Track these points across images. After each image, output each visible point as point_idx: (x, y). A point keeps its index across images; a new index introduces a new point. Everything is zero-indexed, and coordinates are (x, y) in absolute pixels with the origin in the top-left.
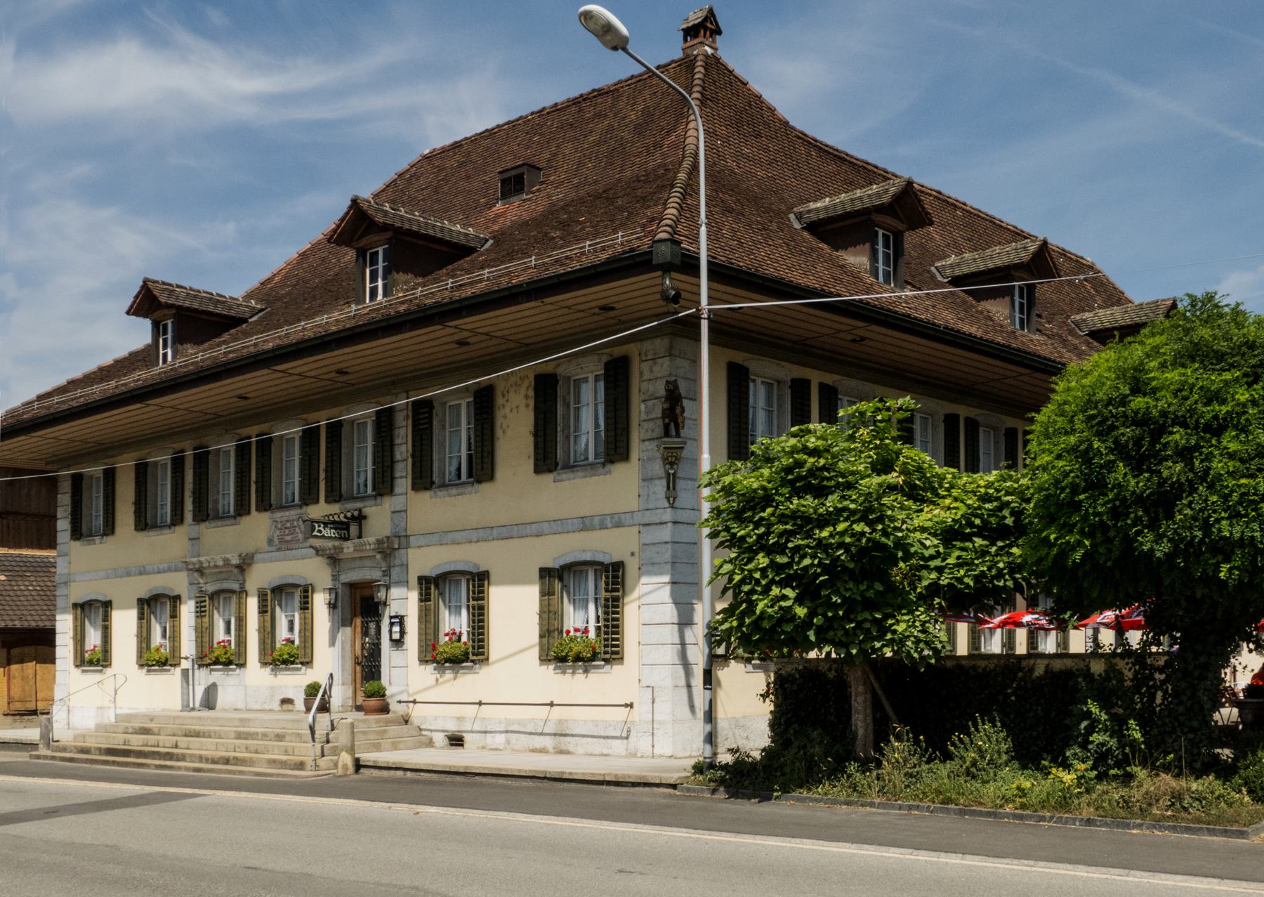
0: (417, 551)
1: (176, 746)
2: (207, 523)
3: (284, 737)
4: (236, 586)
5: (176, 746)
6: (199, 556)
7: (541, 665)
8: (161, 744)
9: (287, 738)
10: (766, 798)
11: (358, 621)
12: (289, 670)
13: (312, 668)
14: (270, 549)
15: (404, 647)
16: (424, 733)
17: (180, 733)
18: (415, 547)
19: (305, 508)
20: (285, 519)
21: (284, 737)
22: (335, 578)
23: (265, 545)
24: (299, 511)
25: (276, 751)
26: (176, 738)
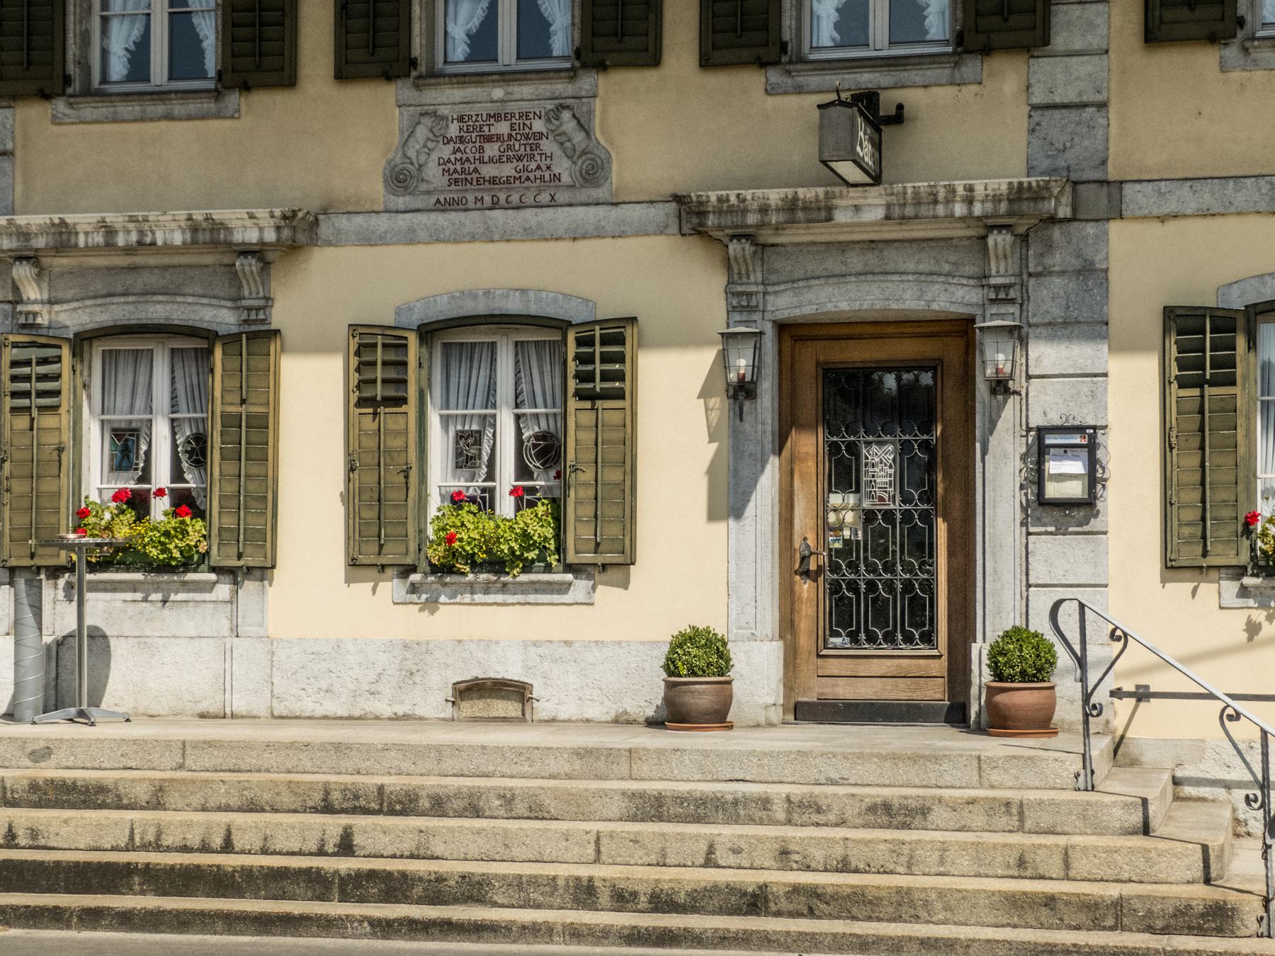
0: (1154, 230)
1: (228, 847)
2: (60, 105)
3: (924, 811)
4: (224, 318)
5: (228, 847)
6: (13, 212)
7: (349, 580)
8: (168, 841)
9: (939, 815)
10: (148, 865)
11: (808, 444)
12: (504, 588)
13: (625, 585)
14: (401, 202)
15: (1094, 524)
16: (1188, 790)
17: (286, 799)
18: (1136, 218)
19: (587, 81)
20: (484, 109)
21: (924, 811)
22: (741, 303)
23: (375, 188)
24: (561, 87)
25: (964, 863)
26: (224, 818)
